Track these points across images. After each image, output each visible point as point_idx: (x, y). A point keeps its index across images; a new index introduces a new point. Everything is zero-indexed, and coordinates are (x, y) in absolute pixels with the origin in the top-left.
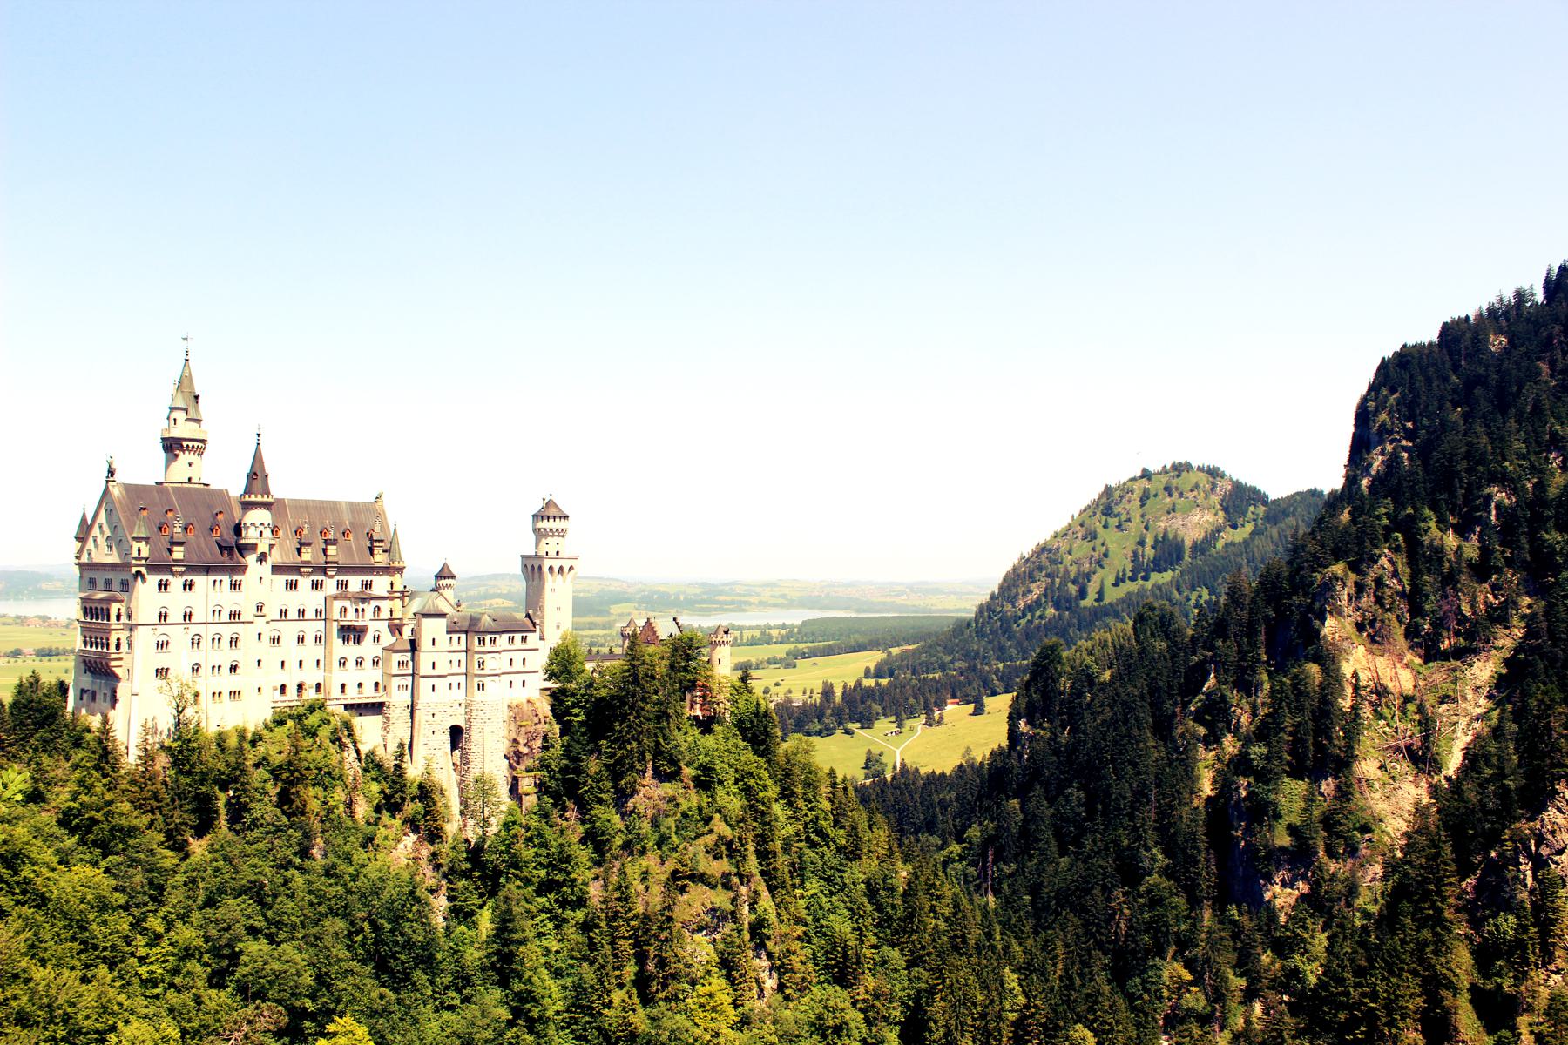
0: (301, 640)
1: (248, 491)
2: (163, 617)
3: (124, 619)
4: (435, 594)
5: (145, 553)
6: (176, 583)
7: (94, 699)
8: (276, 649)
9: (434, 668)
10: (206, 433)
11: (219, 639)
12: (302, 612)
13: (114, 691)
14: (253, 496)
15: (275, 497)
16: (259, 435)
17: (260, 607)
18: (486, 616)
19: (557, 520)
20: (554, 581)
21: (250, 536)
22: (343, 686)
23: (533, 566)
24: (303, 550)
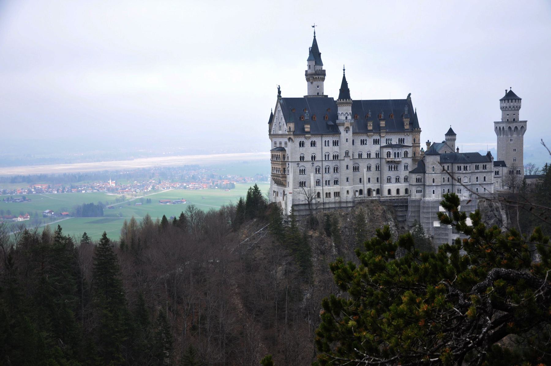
0: (369, 168)
1: (341, 97)
2: (302, 158)
3: (286, 160)
4: (443, 144)
5: (292, 129)
6: (308, 143)
7: (278, 195)
8: (357, 173)
9: (434, 182)
10: (325, 71)
11: (328, 168)
12: (369, 155)
13: (284, 192)
14: (342, 100)
15: (353, 100)
16: (344, 70)
17: (347, 154)
18: (462, 155)
19: (514, 101)
20: (512, 135)
21: (342, 118)
22: (389, 191)
23: (500, 127)
24: (369, 125)
